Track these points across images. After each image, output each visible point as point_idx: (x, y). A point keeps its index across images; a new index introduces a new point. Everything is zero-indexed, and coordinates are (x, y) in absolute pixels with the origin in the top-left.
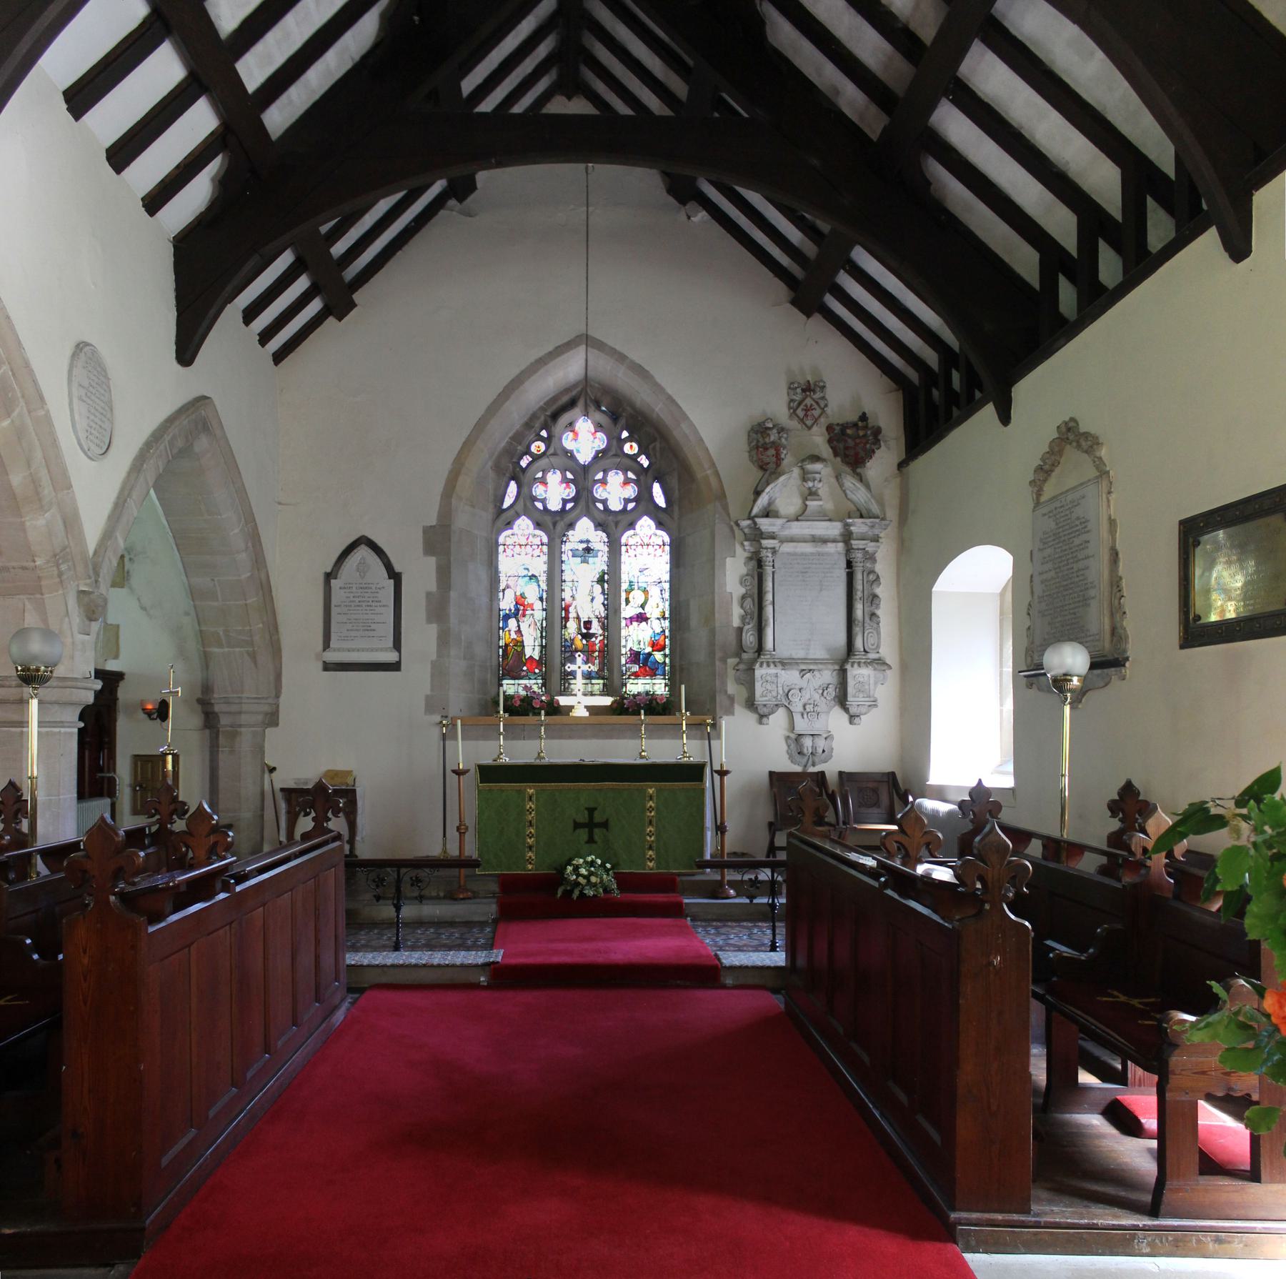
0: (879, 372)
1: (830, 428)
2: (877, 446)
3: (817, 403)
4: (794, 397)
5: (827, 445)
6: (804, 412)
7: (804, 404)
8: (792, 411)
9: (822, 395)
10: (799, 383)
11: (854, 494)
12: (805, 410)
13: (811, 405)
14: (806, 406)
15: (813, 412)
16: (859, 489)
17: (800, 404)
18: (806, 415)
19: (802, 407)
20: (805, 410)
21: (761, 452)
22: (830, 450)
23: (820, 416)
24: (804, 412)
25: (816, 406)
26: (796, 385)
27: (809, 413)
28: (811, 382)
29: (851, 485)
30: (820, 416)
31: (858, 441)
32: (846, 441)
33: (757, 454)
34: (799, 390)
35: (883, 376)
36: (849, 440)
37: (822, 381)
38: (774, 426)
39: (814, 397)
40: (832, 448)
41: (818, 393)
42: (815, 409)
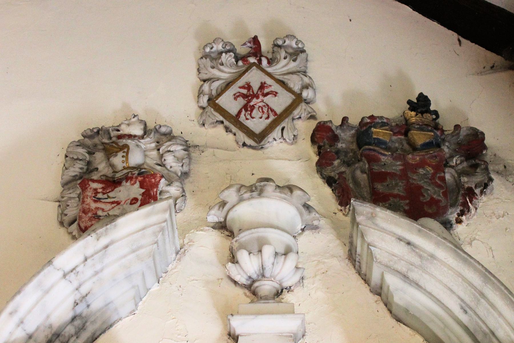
0: (452, 36)
1: (319, 145)
2: (479, 178)
3: (283, 84)
4: (216, 73)
5: (319, 181)
6: (242, 101)
7: (242, 82)
8: (204, 101)
9: (293, 66)
10: (226, 44)
11: (417, 285)
12: (244, 96)
13: (262, 86)
14: (248, 87)
15: (269, 100)
16: (433, 256)
17: (228, 85)
18: (248, 108)
19: (234, 89)
20: (244, 96)
21: (96, 192)
22: (327, 190)
23: (288, 111)
24: (242, 101)
25: (276, 87)
26: (219, 47)
27: (254, 101)
28: (262, 41)
29: (400, 249)
30: (288, 111)
31: (413, 158)
32: (372, 160)
33: (82, 199)
34: (228, 58)
35: (463, 40)
36: (386, 158)
37: (291, 36)
38: (146, 132)
39: (269, 70)
40: (330, 181)
41: (283, 62)
42: (275, 94)
